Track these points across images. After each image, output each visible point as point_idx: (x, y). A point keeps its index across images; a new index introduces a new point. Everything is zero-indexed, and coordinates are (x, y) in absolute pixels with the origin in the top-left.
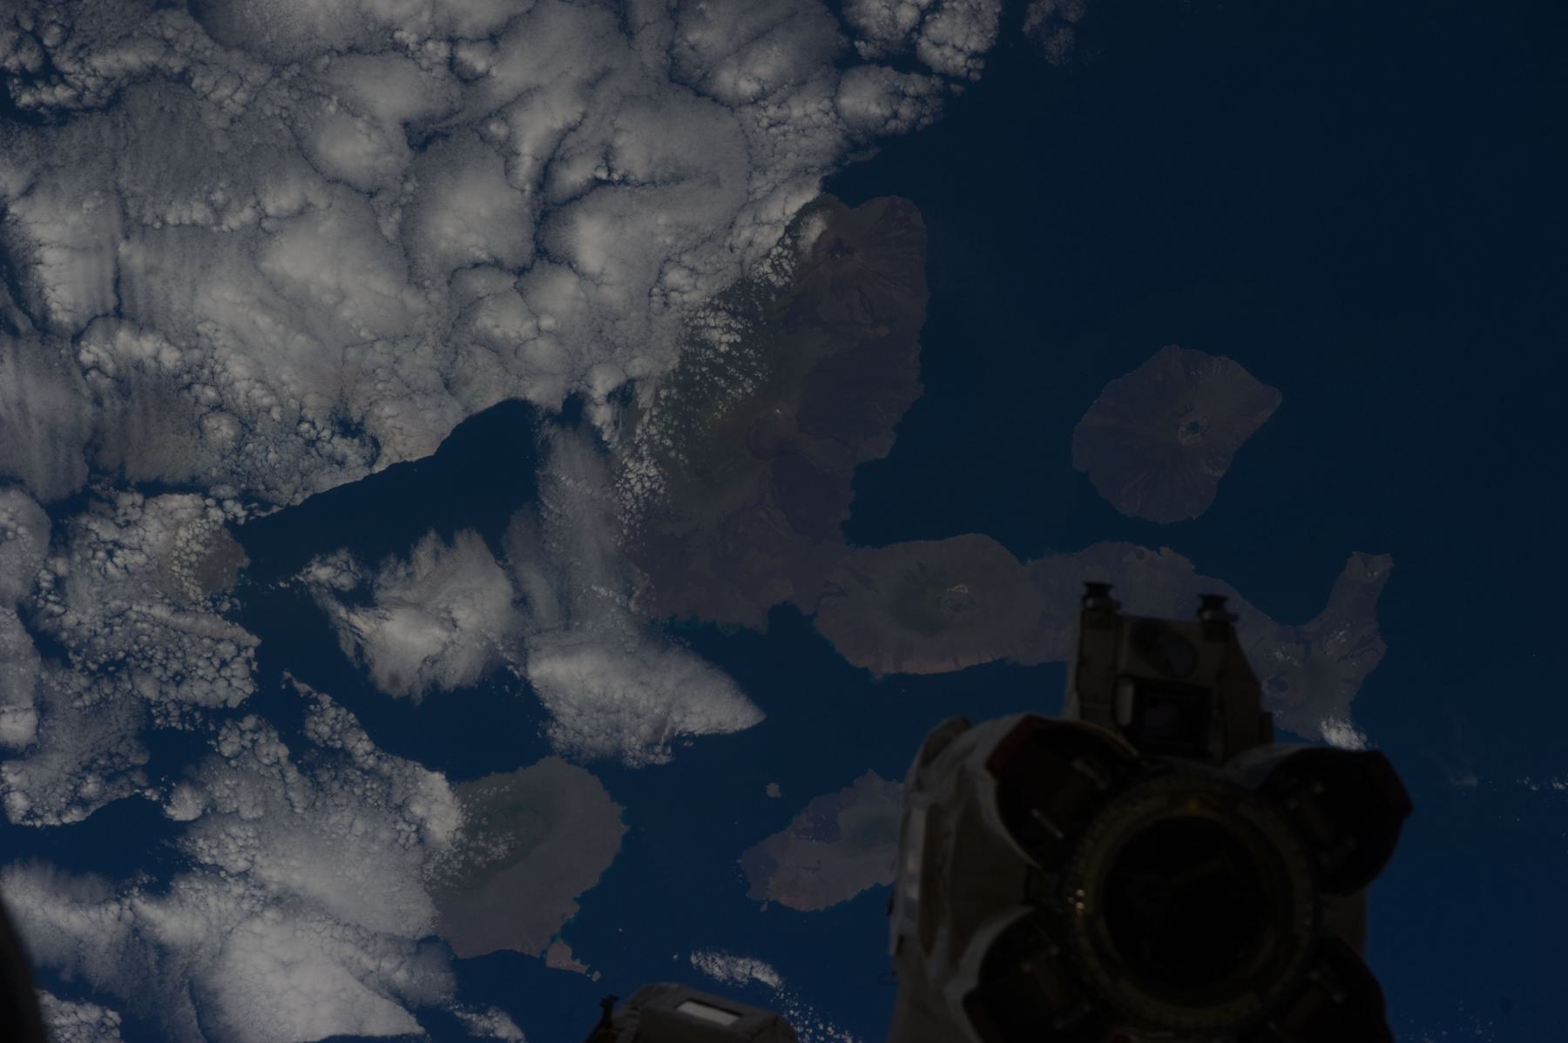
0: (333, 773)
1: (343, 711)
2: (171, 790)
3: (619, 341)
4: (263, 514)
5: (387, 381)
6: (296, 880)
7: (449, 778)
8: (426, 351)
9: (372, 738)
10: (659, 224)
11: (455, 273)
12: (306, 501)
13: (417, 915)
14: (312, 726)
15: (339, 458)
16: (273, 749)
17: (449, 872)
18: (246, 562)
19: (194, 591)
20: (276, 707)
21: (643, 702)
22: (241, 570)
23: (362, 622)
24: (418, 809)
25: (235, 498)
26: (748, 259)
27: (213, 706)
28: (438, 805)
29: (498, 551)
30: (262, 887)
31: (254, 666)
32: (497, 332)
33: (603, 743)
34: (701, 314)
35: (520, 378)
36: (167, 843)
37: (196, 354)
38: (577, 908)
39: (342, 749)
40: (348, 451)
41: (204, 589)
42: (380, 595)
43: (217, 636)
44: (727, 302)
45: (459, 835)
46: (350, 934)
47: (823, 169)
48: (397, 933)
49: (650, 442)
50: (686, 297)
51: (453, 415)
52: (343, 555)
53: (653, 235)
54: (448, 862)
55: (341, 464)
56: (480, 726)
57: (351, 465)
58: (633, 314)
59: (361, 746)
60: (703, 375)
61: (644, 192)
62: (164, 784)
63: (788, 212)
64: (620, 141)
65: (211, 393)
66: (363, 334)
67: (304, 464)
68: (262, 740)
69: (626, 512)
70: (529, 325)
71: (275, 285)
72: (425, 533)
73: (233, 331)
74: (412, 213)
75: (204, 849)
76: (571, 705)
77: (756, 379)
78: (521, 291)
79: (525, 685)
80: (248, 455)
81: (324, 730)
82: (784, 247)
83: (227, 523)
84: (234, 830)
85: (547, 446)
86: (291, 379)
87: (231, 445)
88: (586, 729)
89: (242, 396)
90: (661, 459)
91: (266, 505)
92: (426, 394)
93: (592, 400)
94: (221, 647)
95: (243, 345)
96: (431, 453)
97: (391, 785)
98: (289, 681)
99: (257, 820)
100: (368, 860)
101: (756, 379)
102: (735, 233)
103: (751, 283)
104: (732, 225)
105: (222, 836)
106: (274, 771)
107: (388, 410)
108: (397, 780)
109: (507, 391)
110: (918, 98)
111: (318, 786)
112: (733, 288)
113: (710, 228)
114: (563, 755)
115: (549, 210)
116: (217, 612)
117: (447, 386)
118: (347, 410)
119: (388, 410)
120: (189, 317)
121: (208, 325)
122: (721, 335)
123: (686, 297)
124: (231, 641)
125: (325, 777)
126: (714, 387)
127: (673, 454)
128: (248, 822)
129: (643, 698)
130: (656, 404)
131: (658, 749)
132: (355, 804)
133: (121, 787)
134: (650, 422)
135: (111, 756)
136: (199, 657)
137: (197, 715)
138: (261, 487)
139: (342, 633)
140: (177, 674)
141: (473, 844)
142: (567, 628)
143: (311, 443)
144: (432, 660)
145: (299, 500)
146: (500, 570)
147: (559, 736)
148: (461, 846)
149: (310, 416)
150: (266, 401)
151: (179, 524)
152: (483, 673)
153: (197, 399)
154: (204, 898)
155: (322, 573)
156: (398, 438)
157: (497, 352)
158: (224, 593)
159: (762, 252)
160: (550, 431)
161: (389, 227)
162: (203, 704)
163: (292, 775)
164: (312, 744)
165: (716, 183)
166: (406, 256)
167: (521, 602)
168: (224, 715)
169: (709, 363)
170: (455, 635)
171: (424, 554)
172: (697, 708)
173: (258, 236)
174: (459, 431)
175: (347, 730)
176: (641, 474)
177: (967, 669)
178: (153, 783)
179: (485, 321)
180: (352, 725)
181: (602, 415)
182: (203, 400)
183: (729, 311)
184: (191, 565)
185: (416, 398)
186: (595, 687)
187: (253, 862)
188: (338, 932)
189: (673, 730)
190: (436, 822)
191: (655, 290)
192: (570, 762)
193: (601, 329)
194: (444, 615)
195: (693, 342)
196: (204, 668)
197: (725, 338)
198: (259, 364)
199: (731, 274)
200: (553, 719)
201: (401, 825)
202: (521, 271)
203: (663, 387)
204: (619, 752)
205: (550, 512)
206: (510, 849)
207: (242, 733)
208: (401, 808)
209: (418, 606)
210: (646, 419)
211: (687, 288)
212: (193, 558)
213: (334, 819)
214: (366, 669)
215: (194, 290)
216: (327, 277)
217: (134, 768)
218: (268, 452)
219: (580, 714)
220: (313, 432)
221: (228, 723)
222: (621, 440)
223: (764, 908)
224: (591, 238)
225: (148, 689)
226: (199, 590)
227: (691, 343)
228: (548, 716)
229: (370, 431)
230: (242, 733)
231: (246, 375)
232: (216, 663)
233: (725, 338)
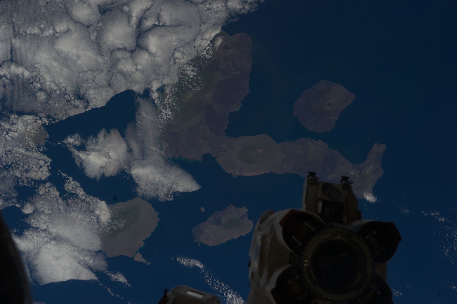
0: (72, 200)
1: (76, 182)
3: (160, 73)
4: (53, 122)
5: (91, 83)
6: (61, 232)
7: (107, 203)
8: (103, 74)
9: (84, 190)
10: (173, 39)
11: (113, 51)
13: (96, 243)
14: (66, 186)
15: (76, 106)
16: (55, 193)
17: (106, 231)
18: (48, 136)
19: (33, 145)
20: (56, 180)
21: (165, 182)
22: (47, 139)
23: (82, 155)
24: (97, 212)
25: (45, 117)
26: (199, 50)
27: (37, 179)
28: (103, 211)
29: (123, 135)
30: (50, 234)
31: (50, 168)
32: (125, 70)
33: (152, 194)
34: (185, 66)
35: (131, 83)
37: (35, 73)
38: (144, 243)
39: (75, 193)
40: (79, 104)
41: (35, 144)
42: (88, 147)
43: (39, 158)
44: (193, 63)
45: (109, 220)
46: (76, 249)
48: (90, 249)
49: (169, 104)
50: (181, 61)
51: (111, 94)
52: (77, 135)
53: (171, 42)
54: (106, 228)
55: (77, 108)
56: (116, 188)
57: (79, 109)
58: (165, 65)
59: (81, 192)
60: (185, 84)
61: (169, 29)
63: (211, 36)
65: (39, 85)
66: (85, 69)
67: (66, 107)
68: (52, 190)
69: (162, 125)
70: (134, 68)
71: (59, 53)
72: (101, 129)
73: (46, 67)
74: (100, 33)
75: (33, 222)
76: (144, 182)
78: (132, 58)
80: (50, 104)
81: (70, 188)
82: (210, 46)
83: (43, 124)
84: (42, 217)
85: (138, 104)
86: (63, 82)
87: (44, 101)
88: (148, 189)
89: (48, 86)
90: (172, 109)
91: (54, 120)
94: (40, 162)
95: (49, 71)
97: (89, 205)
98: (60, 173)
99: (49, 214)
100: (82, 227)
102: (196, 42)
103: (200, 57)
104: (195, 39)
105: (39, 219)
106: (55, 199)
107: (91, 92)
108: (91, 203)
109: (127, 87)
111: (68, 204)
112: (195, 59)
113: (188, 40)
114: (141, 197)
115: (141, 33)
116: (39, 151)
117: (109, 85)
118: (79, 92)
119: (91, 92)
120: (33, 62)
121: (38, 65)
122: (191, 72)
123: (181, 61)
124: (43, 160)
125: (70, 201)
126: (188, 88)
127: (176, 108)
128: (47, 215)
129: (165, 181)
130: (171, 93)
131: (169, 196)
132: (79, 210)
134: (169, 98)
136: (33, 164)
137: (32, 182)
138: (53, 114)
139: (76, 159)
141: (113, 223)
142: (143, 159)
143: (68, 101)
144: (103, 168)
145: (64, 118)
146: (124, 141)
147: (140, 191)
148: (110, 223)
149: (68, 93)
150: (55, 88)
151: (28, 124)
152: (118, 172)
153: (34, 87)
154: (33, 237)
155: (70, 140)
156: (94, 100)
157: (124, 76)
158: (41, 146)
159: (203, 48)
160: (139, 100)
161: (93, 37)
162: (34, 179)
163: (60, 201)
164: (66, 192)
166: (98, 45)
167: (130, 151)
168: (40, 182)
169: (187, 81)
170: (110, 160)
171: (101, 136)
172: (181, 184)
173: (54, 38)
174: (112, 99)
175: (76, 188)
176: (166, 113)
179: (121, 66)
180: (78, 187)
181: (155, 95)
182: (36, 87)
183: (193, 66)
184: (32, 137)
185: (100, 89)
186: (151, 177)
187: (48, 227)
188: (73, 248)
189: (174, 190)
191: (172, 58)
192: (143, 199)
193: (155, 69)
194: (107, 154)
195: (182, 74)
196: (35, 168)
197: (192, 73)
198: (54, 77)
199: (195, 54)
200: (138, 186)
201: (92, 217)
202: (132, 52)
203: (173, 87)
204: (157, 197)
205: (139, 124)
206: (124, 225)
207: (46, 188)
208: (92, 212)
209: (99, 151)
210: (168, 97)
211: (181, 58)
212: (32, 135)
213: (72, 214)
214: (83, 169)
215: (34, 54)
216: (74, 51)
218: (55, 104)
220: (69, 98)
221: (41, 185)
222: (160, 103)
223: (199, 245)
224: (153, 42)
226: (34, 144)
227: (182, 74)
228: (136, 185)
229: (86, 98)
230: (46, 188)
231: (49, 80)
232: (39, 166)
233: (192, 73)
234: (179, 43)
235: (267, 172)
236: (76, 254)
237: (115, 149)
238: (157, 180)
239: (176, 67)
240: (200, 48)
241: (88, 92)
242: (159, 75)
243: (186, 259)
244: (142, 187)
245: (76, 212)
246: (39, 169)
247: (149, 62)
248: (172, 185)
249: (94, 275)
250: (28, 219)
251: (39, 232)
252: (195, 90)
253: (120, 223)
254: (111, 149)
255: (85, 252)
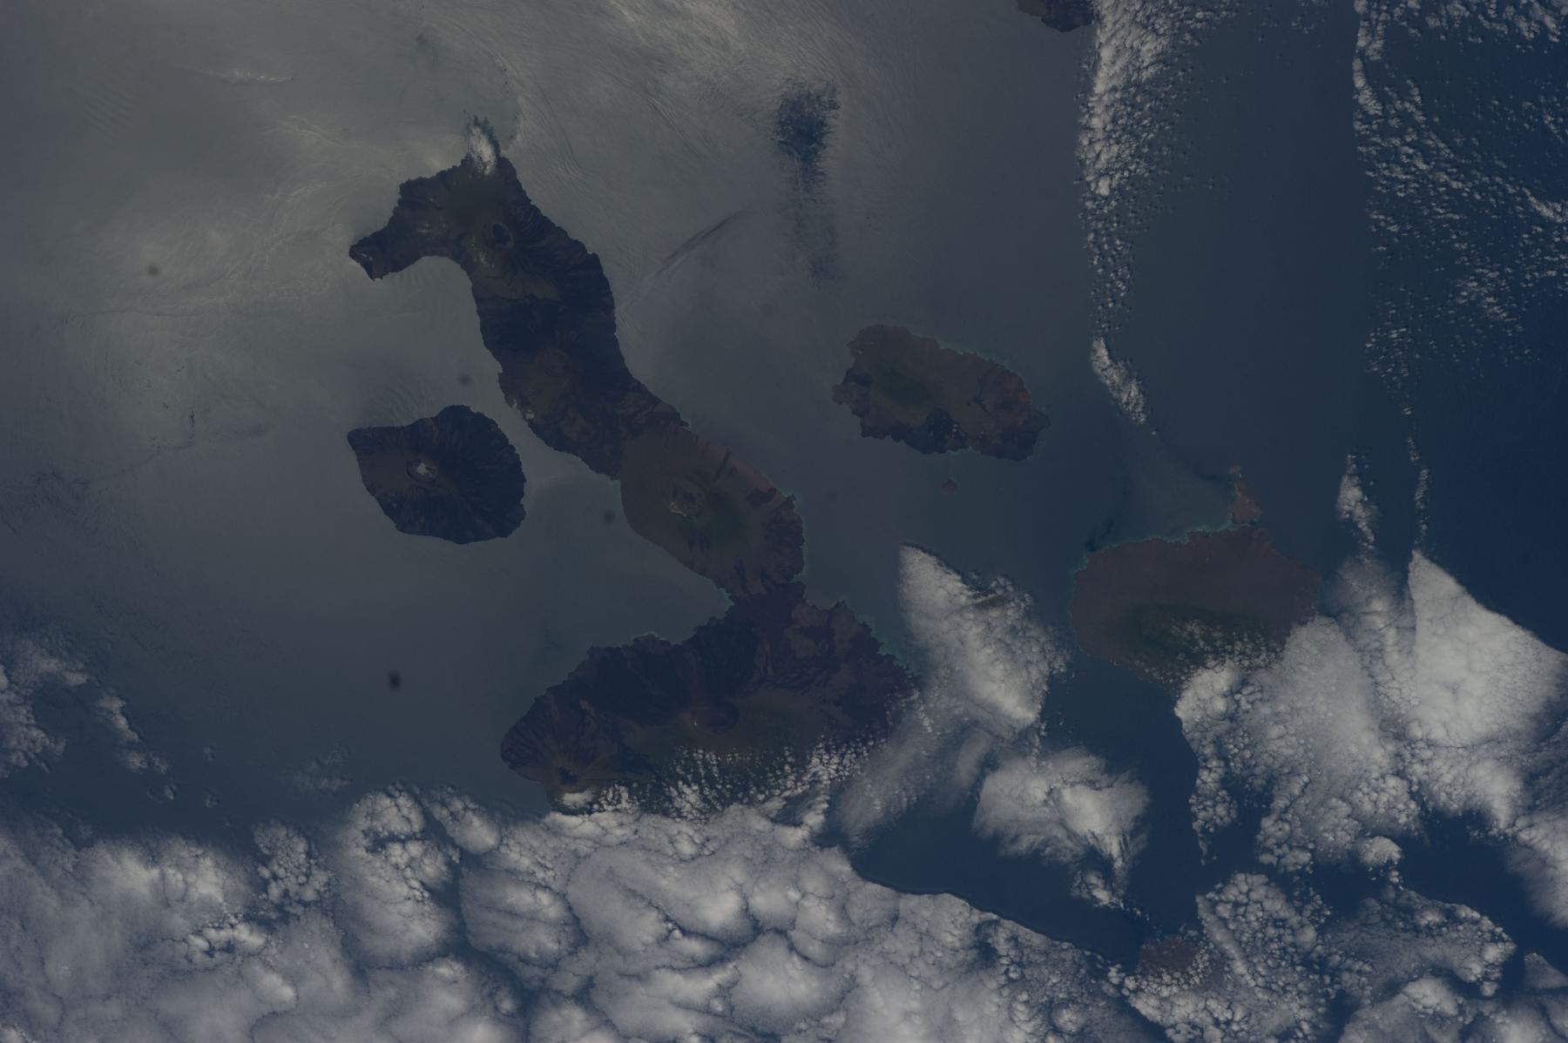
2: (1377, 868)
6: (1366, 738)
7: (1174, 704)
8: (887, 946)
9: (1197, 776)
10: (670, 882)
12: (1062, 941)
13: (1312, 643)
16: (1272, 830)
21: (976, 630)
23: (1113, 847)
24: (1220, 705)
29: (971, 800)
30: (1398, 755)
32: (832, 917)
35: (844, 883)
36: (1428, 841)
40: (1002, 941)
42: (1080, 850)
45: (1211, 663)
46: (1377, 668)
47: (538, 822)
48: (1342, 637)
51: (909, 903)
53: (678, 880)
54: (1242, 653)
56: (1109, 714)
59: (1208, 779)
60: (724, 785)
61: (661, 904)
62: (1377, 875)
64: (650, 939)
68: (1273, 841)
69: (858, 754)
75: (1406, 815)
77: (690, 753)
78: (793, 923)
79: (1043, 715)
81: (1221, 810)
90: (801, 765)
92: (915, 926)
93: (812, 833)
94: (1226, 915)
96: (947, 896)
97: (1219, 737)
99: (1343, 798)
100: (1299, 705)
101: (690, 753)
103: (641, 805)
107: (950, 939)
108: (1210, 736)
109: (861, 883)
110: (444, 805)
111: (1272, 780)
112: (655, 812)
115: (729, 946)
117: (895, 919)
119: (950, 939)
122: (690, 796)
124: (1214, 913)
126: (721, 772)
130: (772, 795)
132: (1259, 748)
133: (1409, 899)
135: (1389, 923)
136: (1248, 923)
140: (1276, 927)
142: (975, 722)
144: (1092, 784)
145: (1065, 945)
146: (982, 796)
155: (1103, 896)
156: (961, 920)
157: (844, 907)
162: (1283, 896)
163: (1280, 803)
165: (611, 871)
167: (989, 764)
168: (1280, 879)
169: (711, 788)
171: (1023, 845)
172: (942, 592)
174: (917, 892)
175: (1207, 797)
178: (1385, 881)
181: (814, 819)
186: (998, 670)
187: (1383, 776)
189: (975, 597)
190: (1217, 687)
193: (765, 862)
195: (710, 810)
197: (688, 791)
199: (650, 820)
200: (1051, 676)
201: (1245, 705)
202: (781, 932)
204: (1028, 614)
205: (909, 797)
208: (1231, 717)
209: (1062, 823)
210: (787, 793)
217: (1382, 902)
219: (1030, 662)
222: (817, 794)
224: (720, 910)
225: (1309, 934)
228: (1052, 680)
230: (1279, 857)
232: (1242, 910)
233: (688, 791)
234: (662, 865)
236: (1393, 658)
237: (1020, 797)
238: (989, 651)
239: (710, 831)
240: (625, 820)
241: (958, 945)
242: (764, 848)
243: (1117, 400)
244: (1044, 667)
245: (1272, 747)
246: (1246, 905)
247: (763, 885)
248: (964, 608)
249: (1411, 565)
250: (1409, 830)
251: (1419, 783)
252: (712, 758)
253: (1192, 634)
254: (1028, 803)
255: (1362, 642)
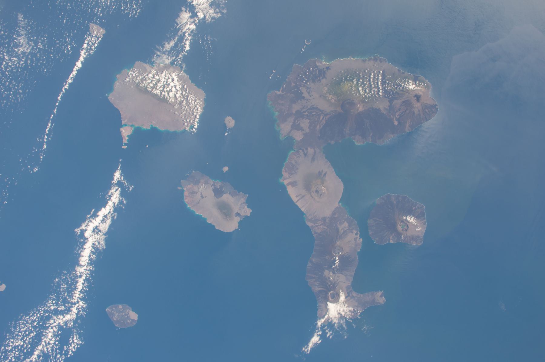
177: (297, 205)
235: (303, 210)
